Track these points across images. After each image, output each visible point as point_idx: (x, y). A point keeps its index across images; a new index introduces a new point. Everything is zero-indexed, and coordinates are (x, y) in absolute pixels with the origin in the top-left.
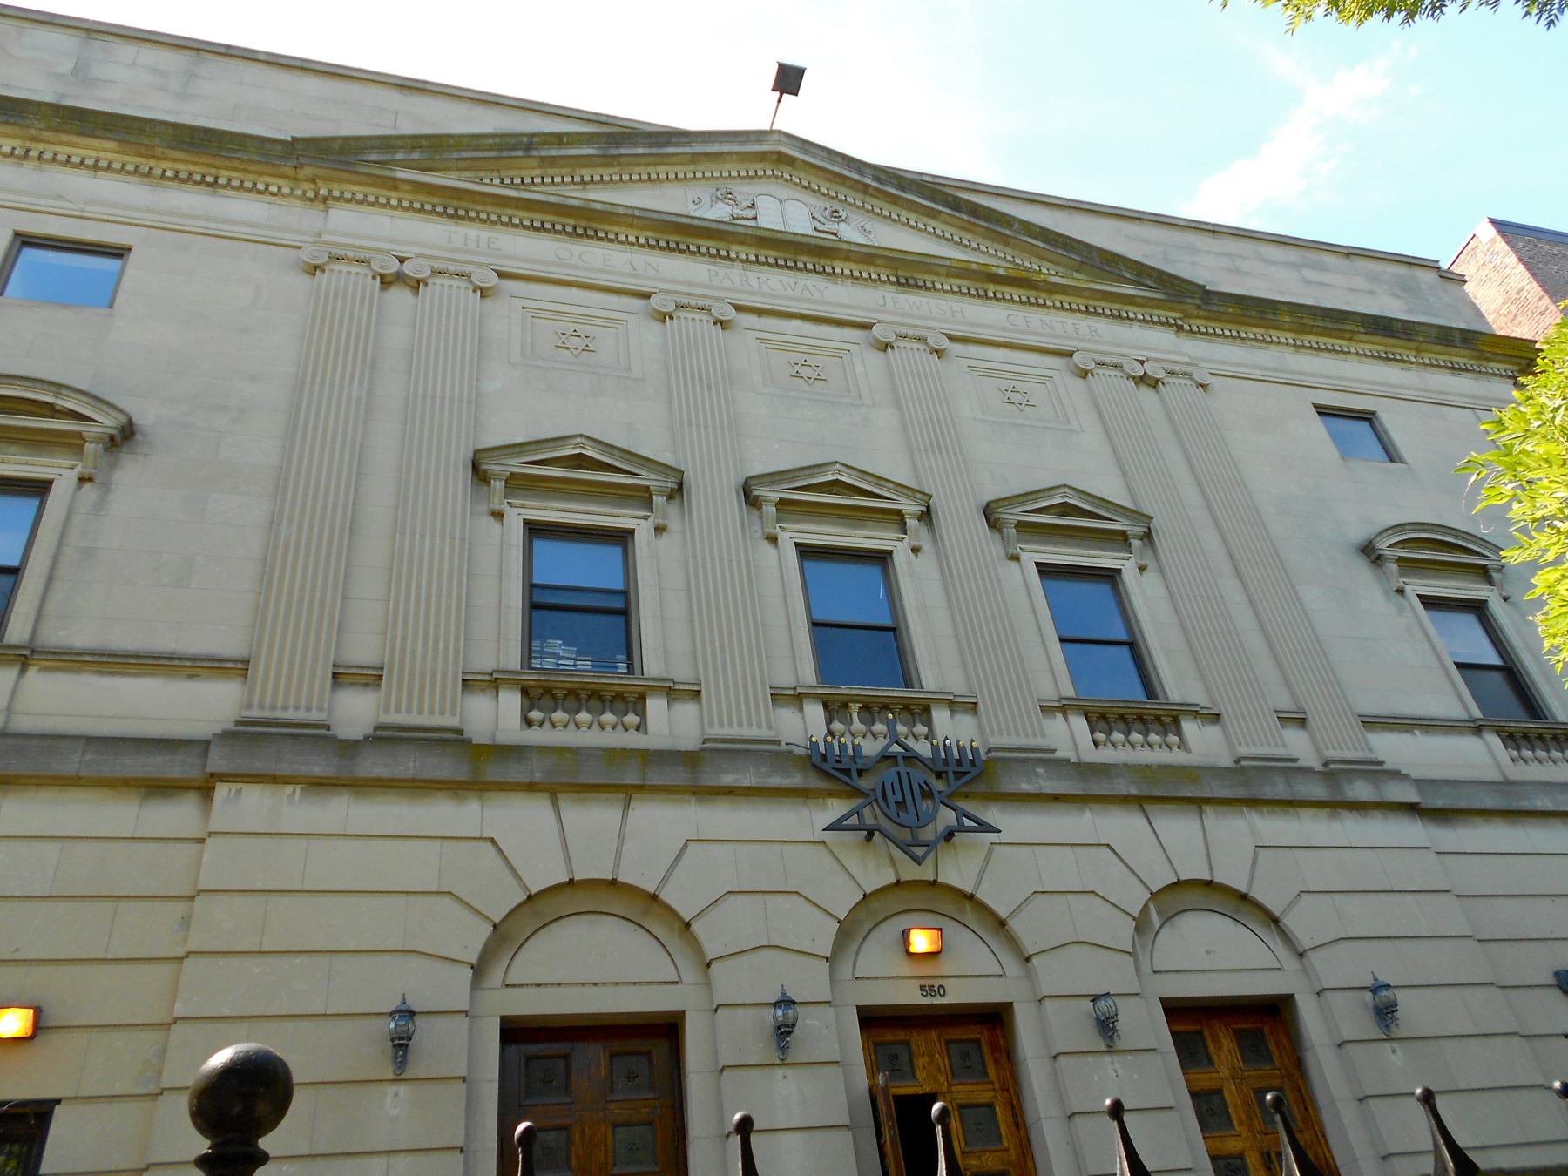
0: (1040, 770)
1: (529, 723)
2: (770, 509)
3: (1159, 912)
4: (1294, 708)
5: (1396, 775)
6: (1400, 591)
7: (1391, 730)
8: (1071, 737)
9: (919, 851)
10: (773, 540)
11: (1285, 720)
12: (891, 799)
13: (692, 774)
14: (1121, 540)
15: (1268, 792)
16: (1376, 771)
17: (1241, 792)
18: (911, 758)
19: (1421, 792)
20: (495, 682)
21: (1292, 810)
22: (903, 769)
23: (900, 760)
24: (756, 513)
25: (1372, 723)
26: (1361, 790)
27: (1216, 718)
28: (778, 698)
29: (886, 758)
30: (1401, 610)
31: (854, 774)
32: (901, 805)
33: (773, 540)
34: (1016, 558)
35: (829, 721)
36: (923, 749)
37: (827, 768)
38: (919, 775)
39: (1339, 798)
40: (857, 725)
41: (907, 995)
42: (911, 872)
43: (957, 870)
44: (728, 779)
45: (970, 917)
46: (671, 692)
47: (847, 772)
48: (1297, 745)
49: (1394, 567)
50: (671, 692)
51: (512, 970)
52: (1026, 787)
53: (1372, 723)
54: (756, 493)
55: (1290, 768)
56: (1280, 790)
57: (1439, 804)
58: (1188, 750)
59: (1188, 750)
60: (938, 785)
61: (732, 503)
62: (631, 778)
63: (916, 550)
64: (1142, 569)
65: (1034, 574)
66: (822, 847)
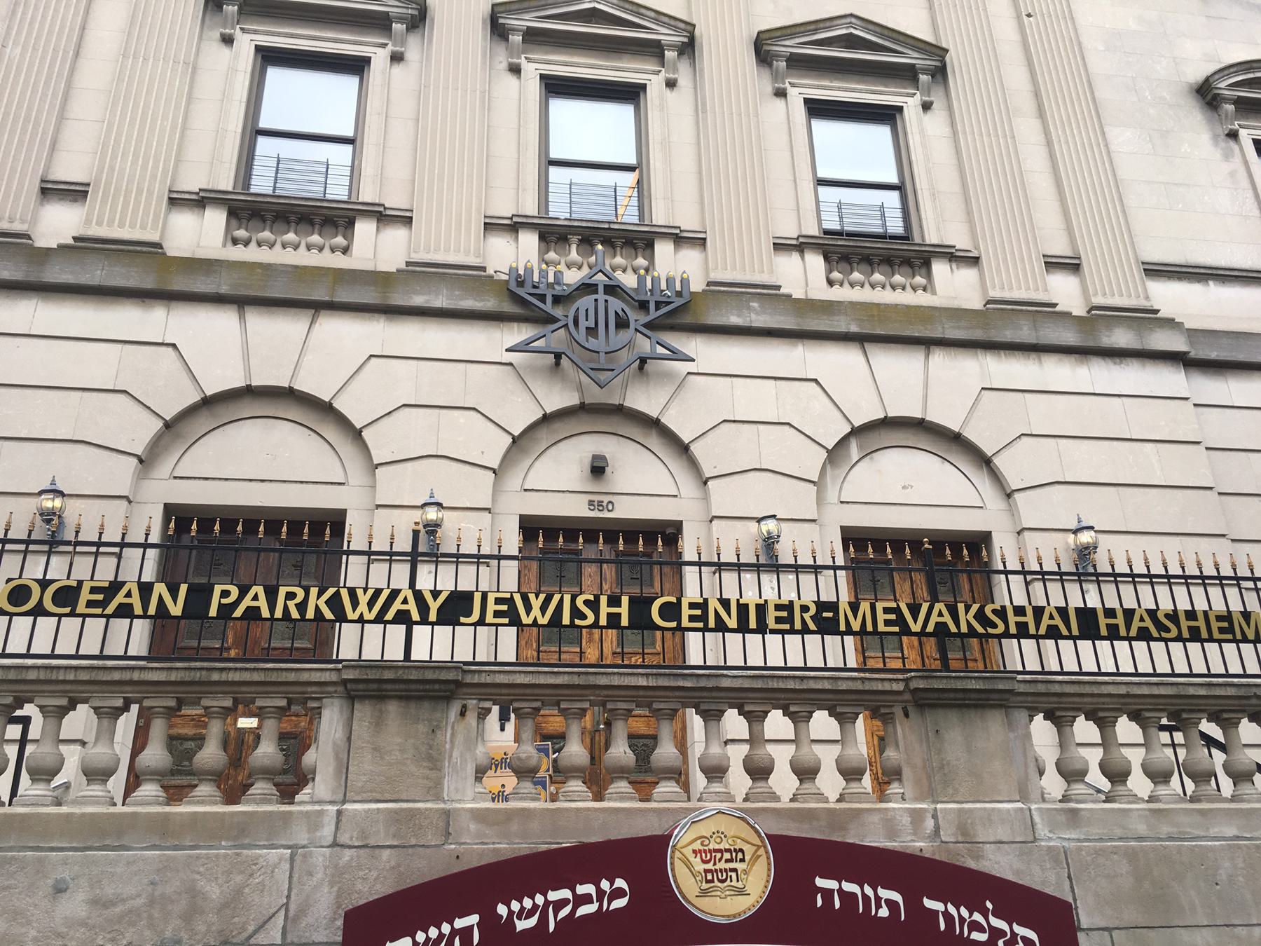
0: (755, 305)
2: (516, 39)
3: (860, 447)
4: (1070, 254)
5: (1170, 323)
6: (1233, 135)
7: (1180, 279)
8: (805, 277)
9: (603, 376)
10: (515, 70)
11: (1053, 264)
12: (583, 324)
13: (380, 298)
14: (907, 75)
15: (1008, 336)
16: (1147, 317)
17: (978, 335)
18: (613, 289)
19: (1191, 343)
20: (201, 201)
21: (1033, 355)
22: (601, 296)
23: (601, 289)
24: (503, 44)
25: (1155, 271)
26: (1121, 338)
27: (975, 261)
28: (491, 227)
29: (587, 288)
30: (1227, 156)
31: (549, 300)
32: (592, 331)
33: (515, 70)
34: (781, 93)
36: (628, 280)
37: (521, 292)
38: (616, 304)
39: (1091, 344)
40: (574, 255)
41: (577, 508)
42: (596, 396)
43: (644, 400)
44: (419, 300)
45: (654, 441)
47: (542, 298)
48: (1065, 292)
49: (1230, 108)
51: (180, 464)
52: (735, 320)
53: (1155, 271)
54: (501, 21)
55: (1045, 311)
56: (1025, 334)
57: (1213, 355)
58: (934, 293)
59: (934, 293)
60: (633, 315)
61: (477, 32)
62: (320, 295)
63: (671, 84)
64: (926, 107)
65: (800, 110)
66: (509, 368)
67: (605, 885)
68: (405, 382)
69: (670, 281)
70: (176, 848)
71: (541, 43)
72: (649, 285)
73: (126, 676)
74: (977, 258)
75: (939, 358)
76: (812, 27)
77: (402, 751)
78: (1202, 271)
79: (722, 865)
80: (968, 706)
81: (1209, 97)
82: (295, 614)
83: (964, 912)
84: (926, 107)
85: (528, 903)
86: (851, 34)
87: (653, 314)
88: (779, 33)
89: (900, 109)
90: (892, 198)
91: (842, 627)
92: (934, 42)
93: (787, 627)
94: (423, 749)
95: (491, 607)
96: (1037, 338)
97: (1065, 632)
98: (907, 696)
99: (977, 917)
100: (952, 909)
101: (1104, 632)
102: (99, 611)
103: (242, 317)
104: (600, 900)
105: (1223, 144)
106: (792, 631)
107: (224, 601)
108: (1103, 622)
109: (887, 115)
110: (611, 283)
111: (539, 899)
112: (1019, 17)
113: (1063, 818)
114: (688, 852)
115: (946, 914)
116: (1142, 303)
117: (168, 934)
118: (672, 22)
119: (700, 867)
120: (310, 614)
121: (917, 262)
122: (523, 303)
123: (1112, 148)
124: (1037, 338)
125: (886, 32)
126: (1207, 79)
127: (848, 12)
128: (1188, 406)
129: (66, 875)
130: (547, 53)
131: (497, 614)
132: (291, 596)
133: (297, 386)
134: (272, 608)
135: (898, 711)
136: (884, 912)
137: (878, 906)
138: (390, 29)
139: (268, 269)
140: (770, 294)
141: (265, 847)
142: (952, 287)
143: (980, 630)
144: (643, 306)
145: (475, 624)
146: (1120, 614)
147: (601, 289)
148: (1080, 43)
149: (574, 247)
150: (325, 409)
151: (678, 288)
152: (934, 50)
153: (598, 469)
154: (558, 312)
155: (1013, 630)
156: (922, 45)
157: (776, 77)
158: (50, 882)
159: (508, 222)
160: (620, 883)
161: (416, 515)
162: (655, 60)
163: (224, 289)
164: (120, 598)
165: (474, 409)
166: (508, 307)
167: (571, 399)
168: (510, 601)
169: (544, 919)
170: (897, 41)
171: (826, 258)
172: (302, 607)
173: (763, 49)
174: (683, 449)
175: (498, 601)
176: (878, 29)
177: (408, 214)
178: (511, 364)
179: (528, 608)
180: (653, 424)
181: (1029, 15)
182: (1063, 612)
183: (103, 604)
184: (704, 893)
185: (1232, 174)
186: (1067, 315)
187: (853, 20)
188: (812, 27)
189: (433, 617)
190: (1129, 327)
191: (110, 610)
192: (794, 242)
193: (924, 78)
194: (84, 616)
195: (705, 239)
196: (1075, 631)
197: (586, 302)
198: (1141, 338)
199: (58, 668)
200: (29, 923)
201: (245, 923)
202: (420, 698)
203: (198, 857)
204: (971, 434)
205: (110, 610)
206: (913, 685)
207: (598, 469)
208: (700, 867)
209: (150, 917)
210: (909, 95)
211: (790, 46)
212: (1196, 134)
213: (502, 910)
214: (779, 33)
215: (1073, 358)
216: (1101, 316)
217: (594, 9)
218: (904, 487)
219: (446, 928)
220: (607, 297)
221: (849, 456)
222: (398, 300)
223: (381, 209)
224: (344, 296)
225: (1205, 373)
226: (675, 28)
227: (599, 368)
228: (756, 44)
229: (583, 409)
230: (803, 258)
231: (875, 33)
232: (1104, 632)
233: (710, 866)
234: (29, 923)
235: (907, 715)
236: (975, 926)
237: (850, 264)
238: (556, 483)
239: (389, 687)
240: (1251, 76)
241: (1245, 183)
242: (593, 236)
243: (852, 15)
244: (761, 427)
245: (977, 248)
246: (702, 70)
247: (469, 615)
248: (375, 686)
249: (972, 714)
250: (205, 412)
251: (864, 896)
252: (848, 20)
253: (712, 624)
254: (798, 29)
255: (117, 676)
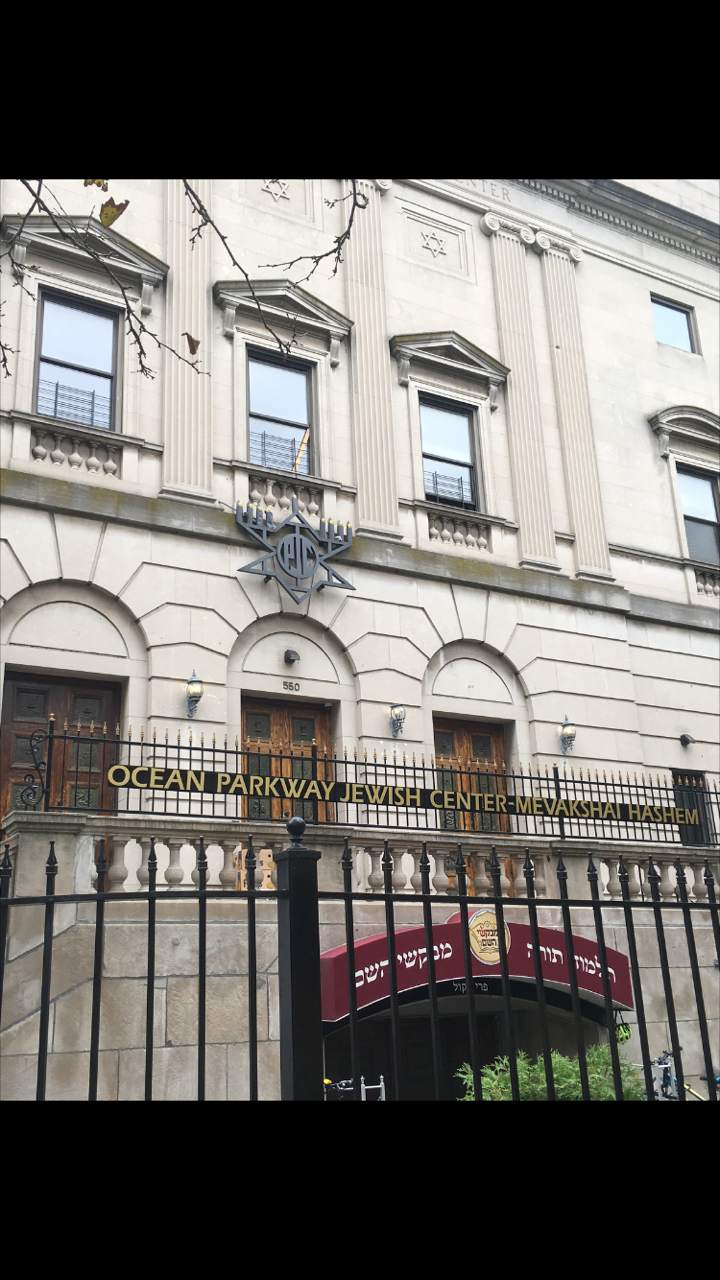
0: (390, 551)
1: (35, 455)
2: (231, 312)
3: (445, 657)
4: (568, 532)
5: (620, 589)
6: (665, 457)
7: (627, 557)
8: (415, 529)
9: (299, 595)
10: (229, 337)
11: (560, 539)
12: (288, 556)
13: (150, 516)
14: (483, 383)
15: (534, 589)
16: (607, 584)
17: (517, 587)
18: (305, 530)
19: (632, 604)
21: (546, 604)
22: (298, 535)
23: (297, 530)
24: (220, 312)
25: (617, 551)
26: (595, 598)
27: (515, 530)
28: (218, 466)
29: (289, 528)
30: (661, 471)
31: (265, 534)
32: (293, 561)
33: (229, 337)
34: (405, 385)
35: (251, 489)
36: (313, 522)
37: (247, 526)
38: (307, 543)
39: (579, 600)
40: (270, 495)
41: (274, 686)
42: (291, 607)
43: (320, 613)
44: (176, 524)
45: (323, 642)
46: (142, 448)
47: (259, 532)
48: (564, 560)
49: (666, 437)
50: (142, 448)
51: (14, 633)
52: (378, 561)
53: (617, 551)
54: (222, 296)
55: (552, 573)
56: (544, 590)
57: (642, 613)
58: (491, 551)
59: (491, 551)
60: (318, 551)
61: (202, 301)
62: (109, 512)
63: (334, 365)
64: (493, 409)
66: (235, 581)
67: (442, 946)
68: (168, 586)
69: (340, 528)
70: (226, 923)
71: (247, 317)
72: (327, 530)
73: (190, 827)
74: (517, 529)
75: (495, 599)
76: (428, 337)
77: (325, 873)
78: (640, 554)
79: (489, 938)
80: (576, 857)
81: (655, 427)
82: (260, 793)
83: (586, 960)
84: (493, 409)
85: (410, 955)
86: (451, 346)
87: (331, 553)
88: (407, 339)
89: (476, 408)
90: (465, 473)
91: (518, 811)
92: (499, 360)
93: (493, 810)
94: (335, 872)
95: (355, 793)
96: (551, 593)
97: (614, 817)
98: (550, 851)
99: (591, 963)
100: (581, 959)
101: (631, 818)
102: (161, 786)
103: (53, 521)
104: (440, 954)
105: (659, 463)
106: (495, 812)
107: (224, 783)
108: (631, 812)
109: (467, 411)
110: (303, 526)
111: (415, 953)
112: (551, 346)
113: (613, 914)
114: (475, 930)
115: (579, 961)
116: (606, 573)
117: (229, 968)
118: (339, 318)
119: (481, 938)
120: (267, 793)
121: (483, 527)
122: (245, 532)
123: (598, 457)
124: (551, 593)
125: (473, 349)
126: (657, 416)
127: (451, 330)
128: (625, 645)
129: (177, 937)
130: (250, 325)
131: (358, 797)
132: (256, 782)
133: (123, 599)
134: (248, 790)
135: (545, 859)
136: (555, 960)
137: (552, 958)
138: (141, 287)
139: (71, 486)
140: (395, 542)
141: (267, 923)
142: (502, 549)
143: (579, 815)
144: (323, 545)
145: (347, 802)
146: (638, 808)
147: (297, 530)
148: (586, 375)
149: (270, 488)
150: (114, 601)
151: (345, 533)
152: (498, 366)
153: (290, 659)
154: (268, 542)
155: (593, 816)
156: (494, 364)
157: (402, 371)
158: (170, 940)
159: (228, 464)
160: (448, 946)
161: (184, 687)
162: (322, 343)
163: (42, 500)
164: (171, 780)
165: (213, 610)
166: (235, 536)
167: (275, 609)
168: (363, 790)
169: (417, 963)
170: (479, 357)
171: (429, 515)
172: (263, 788)
173: (395, 345)
174: (342, 650)
175: (358, 789)
176: (469, 346)
177: (160, 449)
178: (235, 578)
179: (372, 794)
180: (325, 631)
181: (557, 347)
182: (614, 805)
183: (163, 782)
184: (483, 951)
185: (662, 485)
186: (567, 577)
187: (454, 336)
188: (428, 337)
189: (327, 798)
190: (600, 591)
191: (167, 786)
192: (410, 503)
193: (493, 388)
194: (154, 789)
195: (355, 494)
196: (619, 817)
197: (288, 539)
198: (606, 599)
199: (155, 821)
200: (163, 962)
201: (265, 962)
202: (331, 845)
203: (239, 928)
204: (510, 655)
205: (167, 786)
206: (554, 845)
207: (290, 659)
208: (481, 938)
209: (220, 959)
210: (482, 399)
211: (411, 350)
212: (643, 445)
213: (399, 958)
214: (407, 339)
215: (568, 607)
216: (584, 581)
217: (285, 296)
218: (469, 687)
219: (377, 966)
220: (302, 537)
221: (439, 663)
222: (162, 522)
223: (142, 443)
224: (125, 515)
225: (635, 624)
226: (340, 323)
227: (292, 586)
228: (390, 342)
229: (282, 616)
230: (415, 515)
231: (466, 349)
232: (631, 818)
233: (484, 938)
234: (163, 962)
235: (549, 860)
236: (590, 967)
237: (442, 522)
238: (263, 669)
239: (319, 838)
240: (681, 416)
241: (668, 493)
242: (285, 484)
243: (454, 333)
244: (391, 639)
245: (518, 521)
246: (355, 358)
247: (344, 797)
248: (312, 838)
249: (578, 860)
250: (28, 594)
251: (547, 953)
252: (450, 336)
253: (459, 807)
254: (420, 338)
255: (185, 827)
